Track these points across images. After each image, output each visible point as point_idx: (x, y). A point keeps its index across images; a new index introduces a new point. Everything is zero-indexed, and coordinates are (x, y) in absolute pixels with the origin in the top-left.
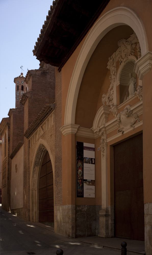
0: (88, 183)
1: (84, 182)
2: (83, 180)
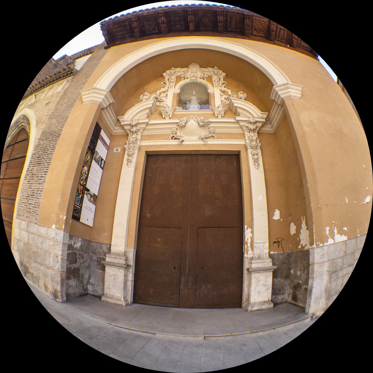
0: (89, 195)
1: (86, 192)
2: (84, 188)
